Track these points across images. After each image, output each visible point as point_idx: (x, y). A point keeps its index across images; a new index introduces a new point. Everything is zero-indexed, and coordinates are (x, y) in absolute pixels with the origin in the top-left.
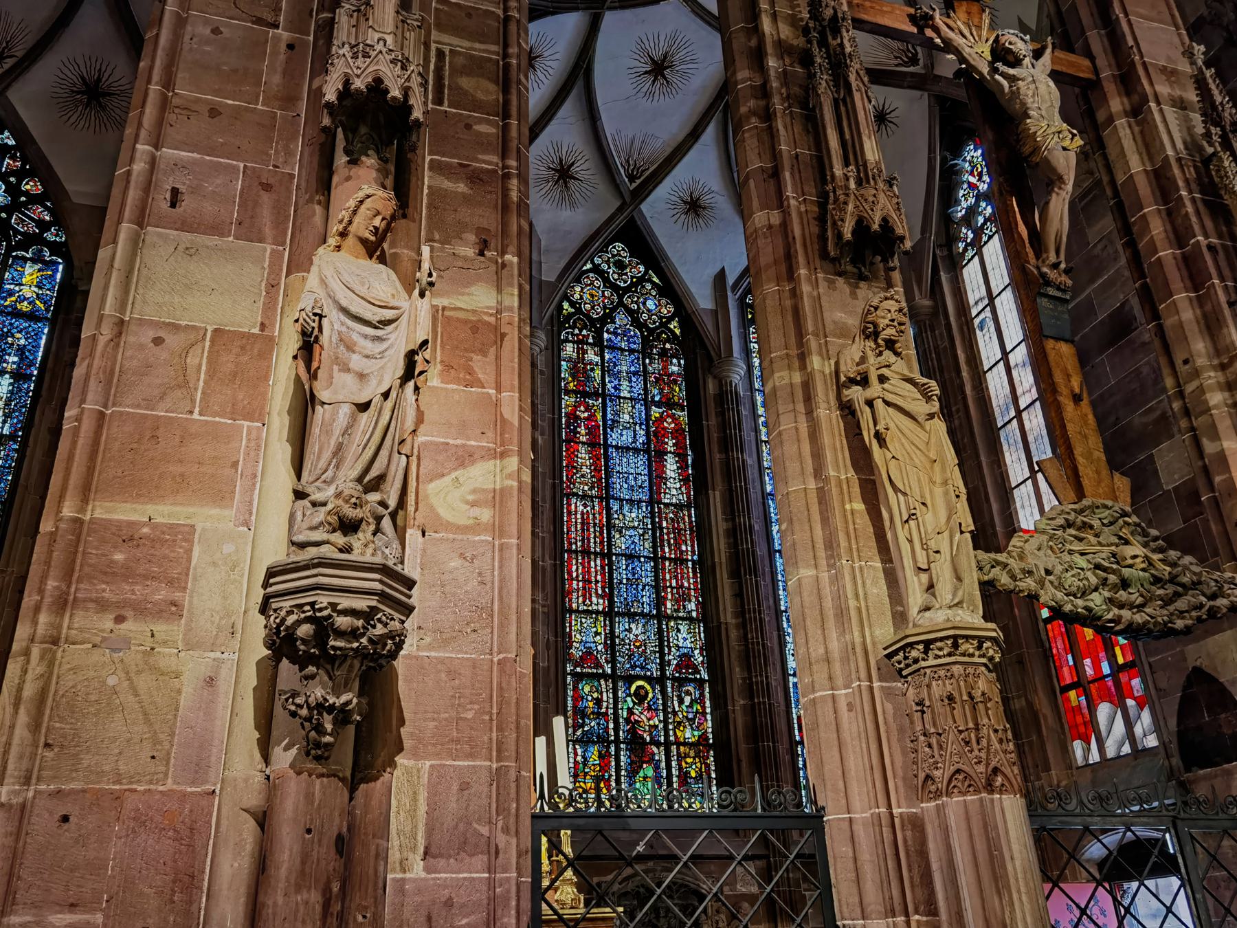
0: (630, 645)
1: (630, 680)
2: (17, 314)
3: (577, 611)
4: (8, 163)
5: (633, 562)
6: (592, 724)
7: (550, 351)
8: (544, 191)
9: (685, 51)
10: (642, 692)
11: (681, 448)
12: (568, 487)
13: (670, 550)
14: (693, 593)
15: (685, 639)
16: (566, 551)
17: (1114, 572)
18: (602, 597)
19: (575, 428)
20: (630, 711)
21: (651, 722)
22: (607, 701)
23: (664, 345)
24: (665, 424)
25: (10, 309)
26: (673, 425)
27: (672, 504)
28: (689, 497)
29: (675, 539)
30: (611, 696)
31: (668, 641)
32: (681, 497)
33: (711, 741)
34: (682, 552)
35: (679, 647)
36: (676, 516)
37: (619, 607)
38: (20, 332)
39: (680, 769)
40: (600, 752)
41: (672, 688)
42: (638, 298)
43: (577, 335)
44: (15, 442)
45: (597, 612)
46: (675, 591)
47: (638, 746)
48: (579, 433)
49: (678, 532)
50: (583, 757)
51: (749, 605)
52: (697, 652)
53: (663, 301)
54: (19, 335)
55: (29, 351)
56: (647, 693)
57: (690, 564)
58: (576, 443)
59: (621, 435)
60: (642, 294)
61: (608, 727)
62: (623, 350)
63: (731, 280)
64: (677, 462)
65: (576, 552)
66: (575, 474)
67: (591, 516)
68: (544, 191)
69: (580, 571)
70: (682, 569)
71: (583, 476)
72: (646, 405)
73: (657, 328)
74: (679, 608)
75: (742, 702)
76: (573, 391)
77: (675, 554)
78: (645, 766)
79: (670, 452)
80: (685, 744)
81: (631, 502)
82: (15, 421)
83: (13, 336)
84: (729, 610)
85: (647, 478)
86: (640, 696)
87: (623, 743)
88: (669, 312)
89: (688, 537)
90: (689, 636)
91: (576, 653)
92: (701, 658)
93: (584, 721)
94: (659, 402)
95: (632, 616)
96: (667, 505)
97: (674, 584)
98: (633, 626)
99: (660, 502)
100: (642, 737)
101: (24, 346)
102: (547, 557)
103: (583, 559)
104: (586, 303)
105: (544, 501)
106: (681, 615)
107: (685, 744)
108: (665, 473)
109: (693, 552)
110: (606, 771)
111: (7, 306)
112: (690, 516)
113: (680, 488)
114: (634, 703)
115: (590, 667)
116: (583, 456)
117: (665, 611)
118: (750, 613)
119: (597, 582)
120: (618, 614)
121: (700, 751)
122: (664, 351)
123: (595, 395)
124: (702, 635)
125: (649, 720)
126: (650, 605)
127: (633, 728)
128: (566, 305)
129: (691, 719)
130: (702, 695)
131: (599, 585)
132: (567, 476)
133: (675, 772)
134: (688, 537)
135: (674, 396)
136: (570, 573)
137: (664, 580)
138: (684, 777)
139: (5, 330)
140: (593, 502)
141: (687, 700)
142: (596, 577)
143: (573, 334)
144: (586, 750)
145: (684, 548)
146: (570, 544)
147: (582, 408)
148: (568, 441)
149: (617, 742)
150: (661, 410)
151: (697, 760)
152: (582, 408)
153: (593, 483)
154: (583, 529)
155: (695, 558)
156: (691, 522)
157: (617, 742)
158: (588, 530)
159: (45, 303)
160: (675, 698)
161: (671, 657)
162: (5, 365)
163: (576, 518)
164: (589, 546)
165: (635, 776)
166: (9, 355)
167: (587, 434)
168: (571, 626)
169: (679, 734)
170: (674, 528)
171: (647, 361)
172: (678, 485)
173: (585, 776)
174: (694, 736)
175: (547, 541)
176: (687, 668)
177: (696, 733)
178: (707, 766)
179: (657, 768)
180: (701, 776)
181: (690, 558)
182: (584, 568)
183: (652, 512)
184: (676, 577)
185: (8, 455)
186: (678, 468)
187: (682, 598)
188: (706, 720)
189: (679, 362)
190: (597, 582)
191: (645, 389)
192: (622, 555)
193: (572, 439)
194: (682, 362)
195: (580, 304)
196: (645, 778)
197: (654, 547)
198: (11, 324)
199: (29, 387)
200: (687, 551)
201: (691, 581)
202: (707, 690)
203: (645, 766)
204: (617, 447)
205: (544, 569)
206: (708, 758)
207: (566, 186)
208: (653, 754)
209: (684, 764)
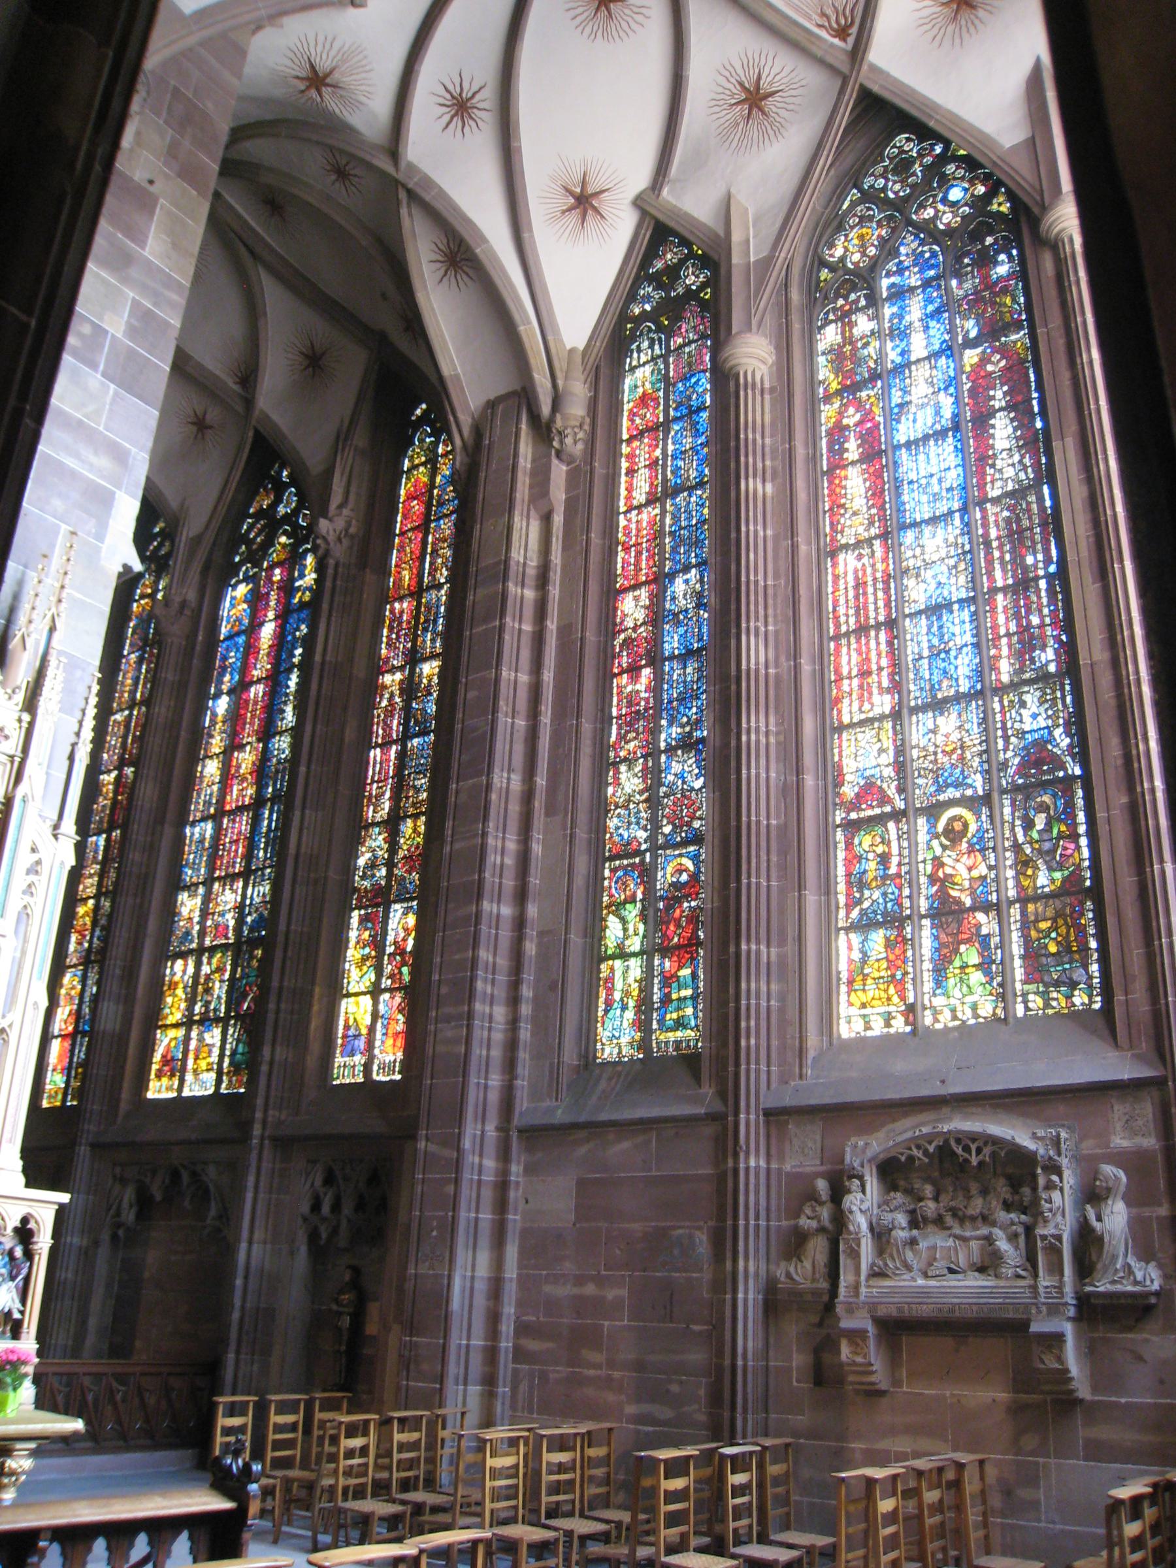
0: (935, 753)
1: (933, 811)
3: (852, 725)
5: (940, 618)
10: (958, 826)
12: (833, 539)
13: (1004, 571)
14: (1049, 631)
15: (1035, 716)
16: (831, 639)
18: (889, 691)
20: (938, 863)
21: (975, 873)
22: (900, 855)
24: (990, 368)
26: (1003, 363)
27: (1007, 495)
29: (1013, 551)
30: (905, 844)
31: (1004, 728)
32: (1022, 476)
33: (1088, 883)
34: (1025, 568)
35: (1024, 733)
36: (1012, 511)
37: (915, 694)
40: (887, 939)
41: (1013, 804)
42: (935, 196)
43: (842, 306)
45: (882, 718)
52: (1058, 732)
56: (966, 825)
57: (1043, 584)
59: (914, 421)
61: (900, 895)
62: (912, 290)
64: (1012, 420)
65: (847, 634)
66: (843, 515)
67: (869, 570)
69: (853, 662)
70: (1027, 598)
71: (855, 514)
74: (1023, 664)
78: (963, 948)
79: (1001, 409)
80: (1036, 899)
81: (934, 520)
85: (960, 469)
86: (953, 835)
90: (1042, 710)
91: (849, 791)
92: (1068, 740)
93: (862, 894)
95: (938, 706)
97: (1013, 627)
98: (941, 720)
99: (982, 501)
100: (958, 902)
102: (783, 659)
103: (858, 641)
106: (1027, 676)
107: (1036, 899)
108: (992, 447)
109: (1048, 561)
110: (898, 968)
113: (1020, 462)
114: (944, 848)
115: (872, 807)
116: (855, 483)
117: (998, 680)
119: (880, 669)
120: (915, 710)
123: (874, 376)
124: (1069, 699)
125: (970, 869)
126: (969, 677)
128: (825, 274)
129: (1048, 852)
130: (1070, 805)
131: (885, 673)
132: (832, 524)
134: (1038, 537)
136: (838, 671)
137: (995, 627)
140: (871, 546)
141: (1040, 821)
142: (878, 663)
144: (865, 940)
145: (1030, 560)
148: (830, 472)
150: (980, 350)
151: (1060, 922)
152: (851, 410)
153: (872, 517)
154: (857, 597)
155: (1052, 569)
158: (865, 594)
160: (1018, 822)
161: (1010, 754)
163: (846, 583)
164: (867, 618)
165: (945, 969)
168: (840, 756)
170: (1010, 534)
172: (1017, 458)
173: (864, 980)
174: (1053, 881)
176: (1038, 763)
177: (1058, 875)
180: (1069, 950)
181: (1041, 573)
182: (860, 654)
186: (1015, 429)
187: (1027, 642)
188: (1078, 848)
190: (880, 669)
192: (920, 612)
193: (838, 464)
194: (1014, 252)
200: (1037, 562)
201: (1046, 611)
202: (1080, 793)
203: (963, 948)
204: (908, 444)
206: (1082, 914)
207: (764, 113)
208: (978, 926)
209: (1033, 934)
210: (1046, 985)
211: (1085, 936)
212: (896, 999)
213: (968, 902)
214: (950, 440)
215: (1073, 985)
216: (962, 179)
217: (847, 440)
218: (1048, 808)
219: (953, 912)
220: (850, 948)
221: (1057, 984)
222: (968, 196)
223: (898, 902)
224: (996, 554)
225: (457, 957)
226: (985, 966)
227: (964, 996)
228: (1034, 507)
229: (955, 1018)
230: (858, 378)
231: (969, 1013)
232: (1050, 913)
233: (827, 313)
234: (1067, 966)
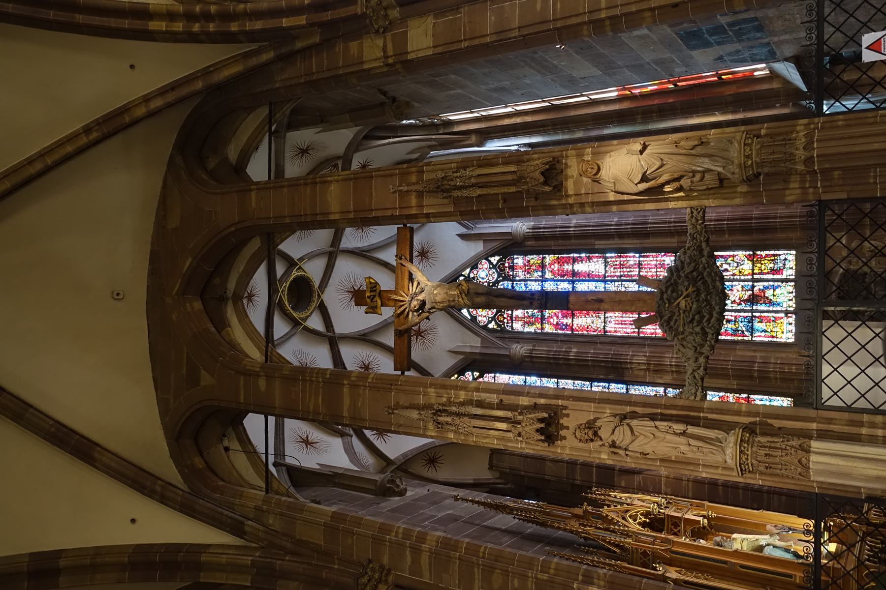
6: (742, 326)
7: (520, 340)
8: (430, 344)
9: (344, 282)
11: (569, 260)
12: (600, 332)
14: (658, 259)
17: (694, 316)
19: (564, 325)
23: (506, 267)
28: (600, 257)
29: (627, 268)
36: (612, 266)
39: (768, 273)
43: (507, 320)
46: (659, 270)
47: (753, 299)
48: (567, 323)
49: (622, 266)
50: (762, 332)
51: (666, 230)
53: (480, 266)
57: (641, 259)
58: (573, 325)
60: (478, 279)
63: (463, 230)
68: (430, 344)
70: (645, 265)
71: (593, 322)
72: (545, 281)
73: (497, 271)
75: (727, 236)
76: (542, 325)
77: (636, 268)
79: (573, 267)
80: (753, 270)
84: (669, 240)
87: (752, 307)
88: (486, 263)
89: (625, 259)
94: (542, 273)
96: (606, 272)
100: (750, 296)
102: (644, 350)
104: (488, 314)
105: (611, 350)
107: (753, 270)
109: (634, 257)
112: (611, 257)
118: (671, 230)
121: (757, 260)
122: (510, 267)
127: (744, 301)
129: (738, 265)
130: (722, 257)
133: (770, 277)
134: (625, 259)
135: (537, 263)
138: (774, 271)
143: (508, 323)
146: (634, 332)
147: (551, 320)
149: (752, 311)
150: (547, 272)
151: (762, 262)
154: (625, 324)
155: (637, 255)
156: (615, 257)
157: (752, 311)
158: (625, 321)
167: (567, 319)
169: (746, 273)
171: (517, 278)
172: (593, 263)
174: (748, 263)
175: (635, 350)
178: (766, 256)
179: (767, 288)
180: (772, 260)
183: (612, 281)
184: (650, 268)
186: (582, 263)
189: (516, 258)
191: (536, 280)
195: (489, 318)
196: (774, 296)
197: (633, 281)
201: (652, 259)
205: (651, 352)
206: (761, 255)
207: (425, 331)
210: (784, 268)
211: (769, 255)
212: (782, 320)
213: (751, 292)
214: (577, 286)
215: (786, 259)
216: (478, 271)
217: (562, 323)
218: (722, 264)
219: (753, 298)
220: (760, 336)
221: (784, 265)
222: (486, 270)
223: (745, 317)
224: (626, 273)
225: (741, 498)
226: (774, 288)
227: (784, 296)
228: (613, 259)
229: (792, 300)
230: (539, 316)
231: (791, 295)
232: (759, 265)
233: (507, 326)
234: (779, 261)
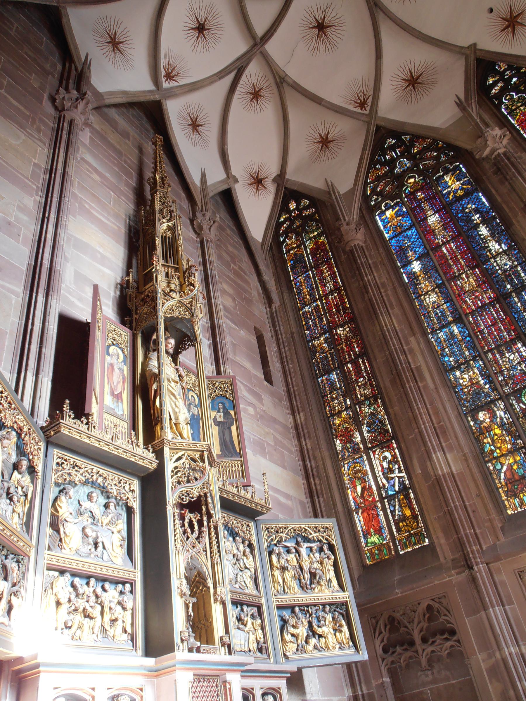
2: (461, 198)
4: (399, 151)
25: (454, 199)
38: (468, 204)
44: (515, 249)
54: (469, 206)
55: (481, 208)
82: (505, 241)
83: (467, 208)
101: (476, 207)
111: (452, 199)
139: (461, 208)
159: (468, 184)
162: (475, 222)
166: (473, 216)
185: (516, 258)
198: (461, 204)
199: (497, 222)
